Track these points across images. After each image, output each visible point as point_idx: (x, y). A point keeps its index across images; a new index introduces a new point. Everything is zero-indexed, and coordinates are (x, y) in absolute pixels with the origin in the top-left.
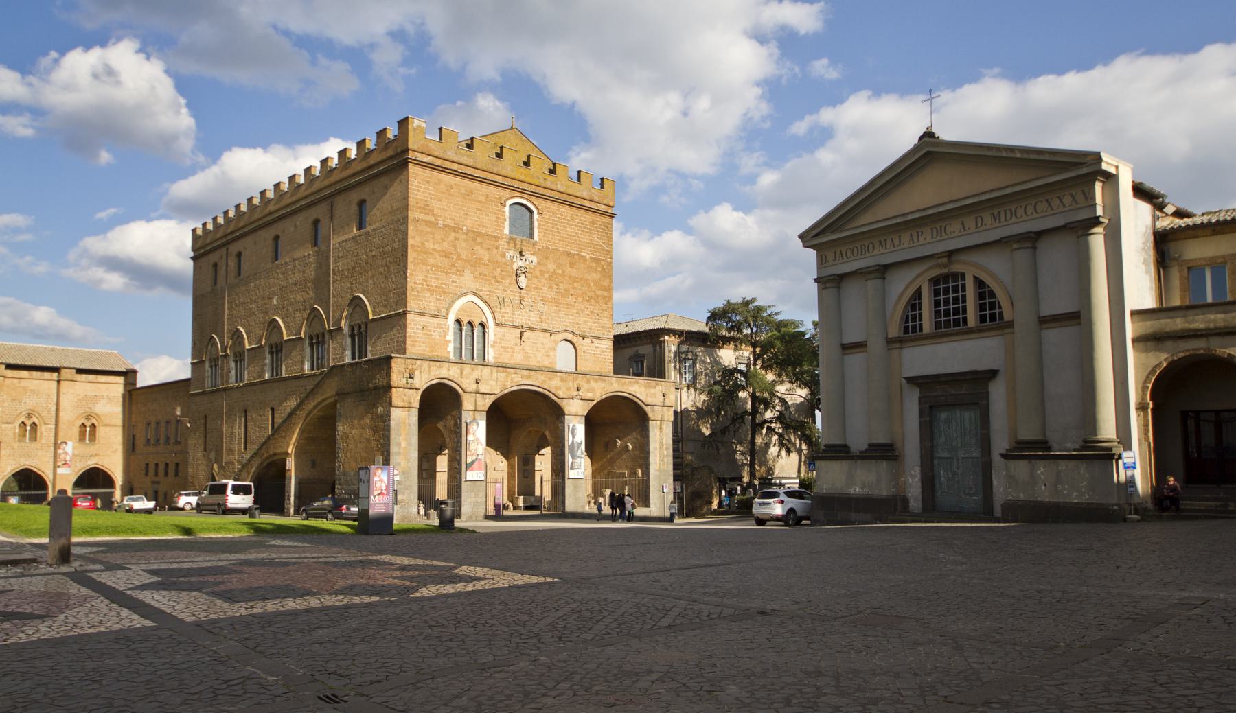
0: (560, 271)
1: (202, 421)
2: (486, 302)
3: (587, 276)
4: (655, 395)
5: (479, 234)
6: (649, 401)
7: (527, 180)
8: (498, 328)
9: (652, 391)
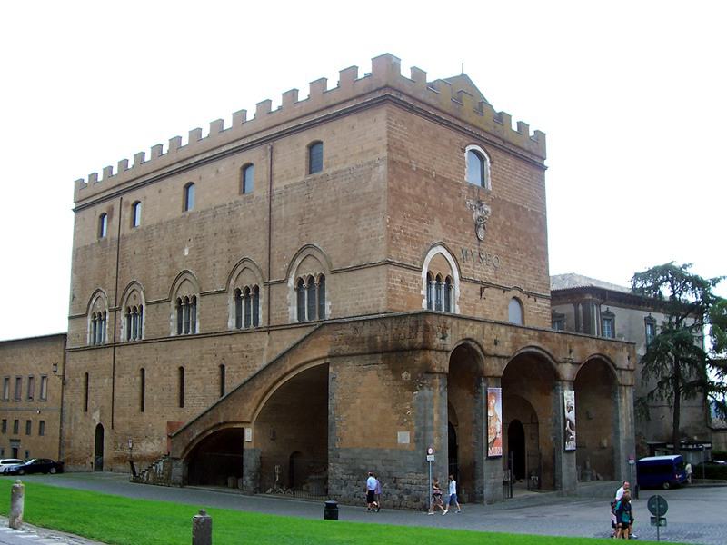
1: (83, 379)
2: (452, 254)
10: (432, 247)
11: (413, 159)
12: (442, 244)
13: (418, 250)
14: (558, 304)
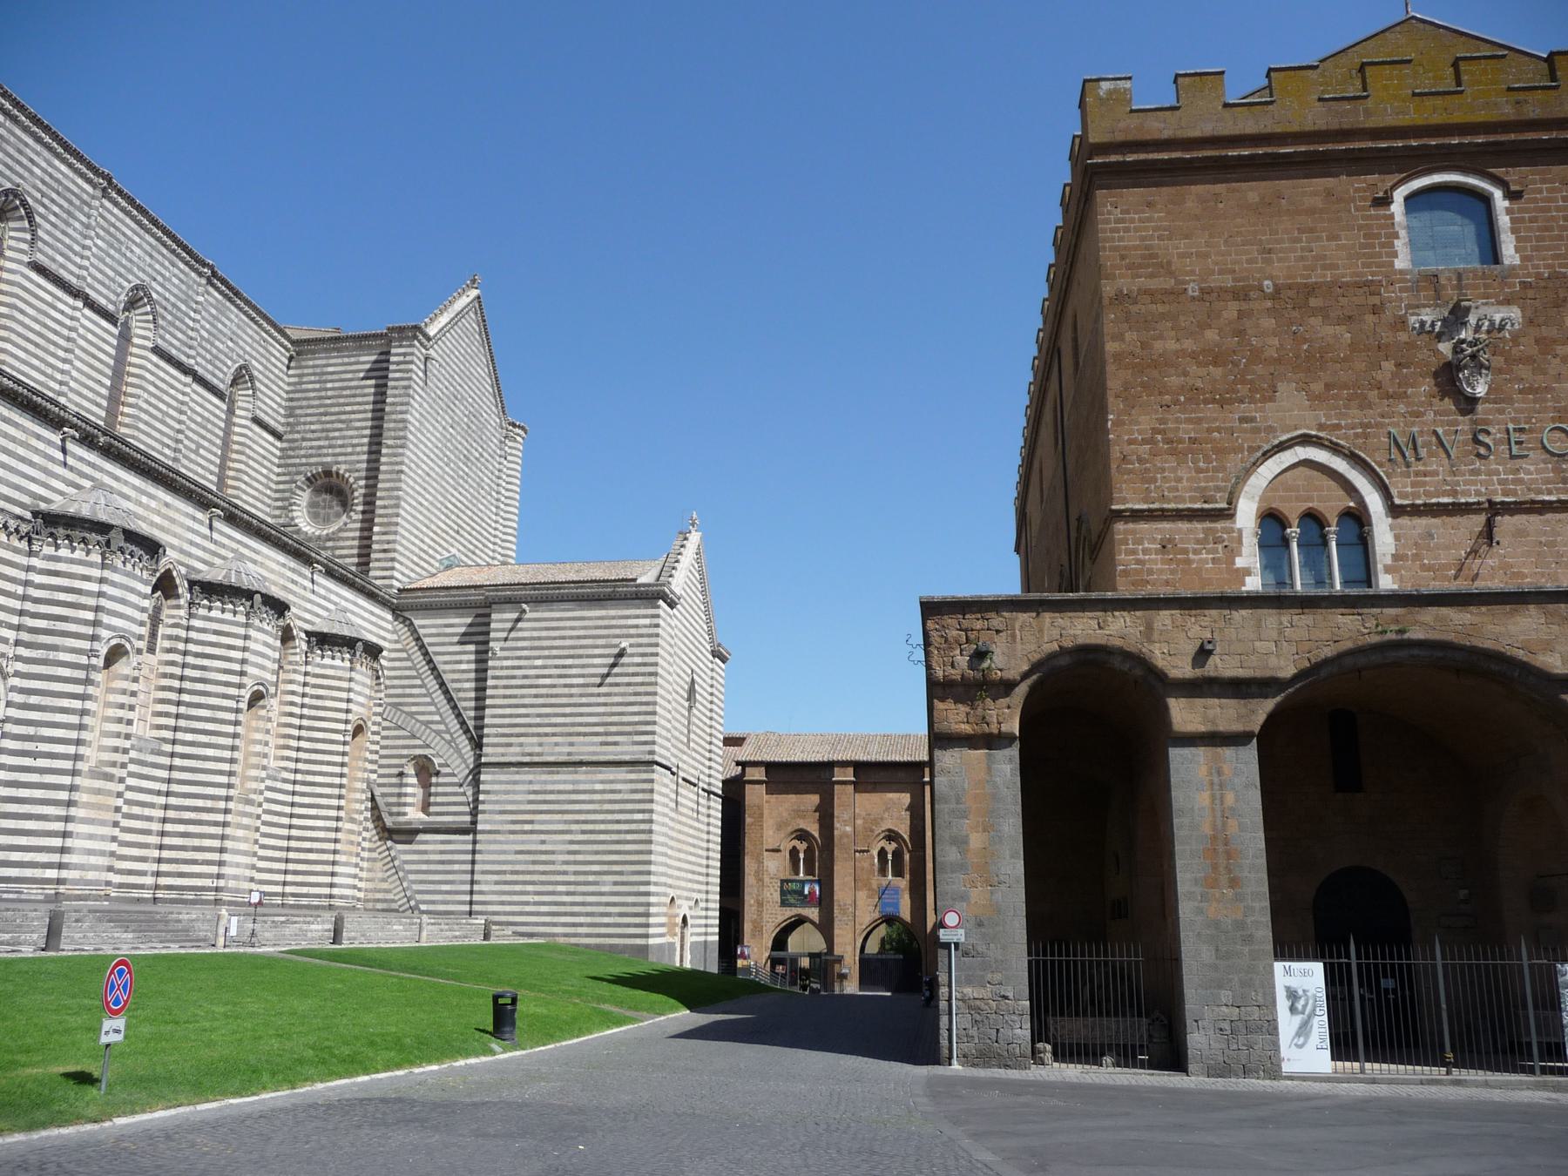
5: (1311, 290)
7: (1458, 117)
8: (1404, 521)
10: (1267, 455)
11: (1192, 272)
12: (1306, 440)
13: (1215, 470)
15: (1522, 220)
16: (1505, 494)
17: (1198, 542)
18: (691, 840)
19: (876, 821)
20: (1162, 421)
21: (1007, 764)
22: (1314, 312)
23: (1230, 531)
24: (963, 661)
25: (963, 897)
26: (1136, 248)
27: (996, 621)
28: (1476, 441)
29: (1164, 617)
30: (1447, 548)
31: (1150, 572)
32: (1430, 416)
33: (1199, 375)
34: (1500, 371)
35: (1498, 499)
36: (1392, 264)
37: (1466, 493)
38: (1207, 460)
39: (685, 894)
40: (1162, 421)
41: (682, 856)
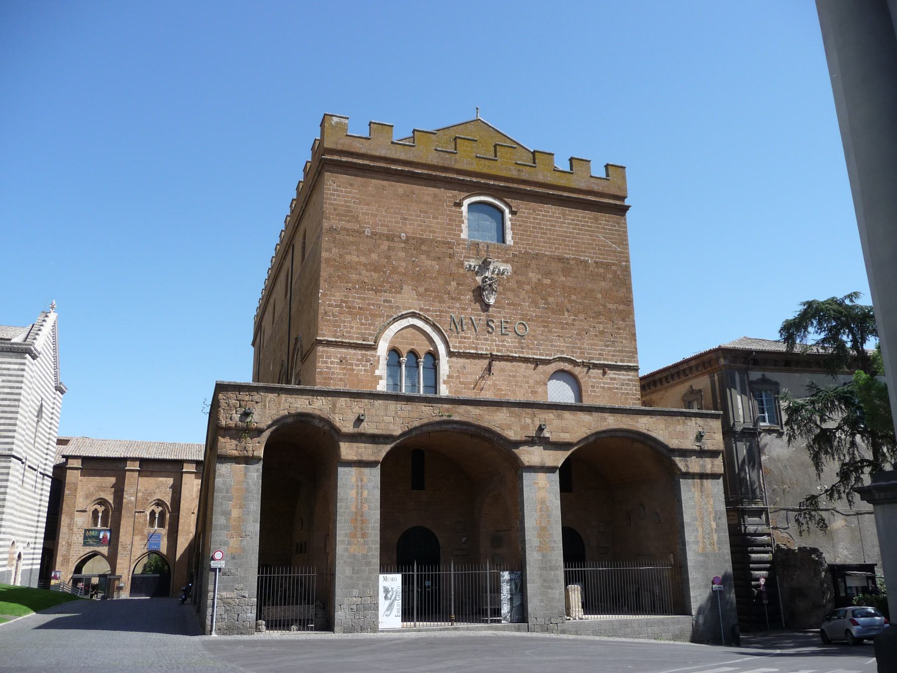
0: (548, 281)
3: (589, 286)
4: (683, 435)
5: (423, 241)
6: (674, 443)
7: (493, 172)
8: (454, 359)
9: (679, 428)
10: (395, 320)
11: (368, 223)
12: (414, 315)
13: (370, 325)
14: (696, 377)
15: (515, 225)
16: (498, 351)
17: (358, 360)
18: (29, 505)
19: (150, 494)
20: (346, 296)
21: (255, 473)
22: (423, 252)
23: (374, 356)
24: (237, 417)
25: (226, 544)
26: (342, 206)
27: (257, 397)
28: (488, 325)
29: (342, 401)
30: (471, 374)
31: (333, 373)
32: (469, 310)
33: (367, 276)
34: (501, 294)
35: (495, 353)
36: (460, 235)
37: (482, 349)
38: (366, 319)
39: (22, 539)
40: (346, 296)
41: (23, 515)
